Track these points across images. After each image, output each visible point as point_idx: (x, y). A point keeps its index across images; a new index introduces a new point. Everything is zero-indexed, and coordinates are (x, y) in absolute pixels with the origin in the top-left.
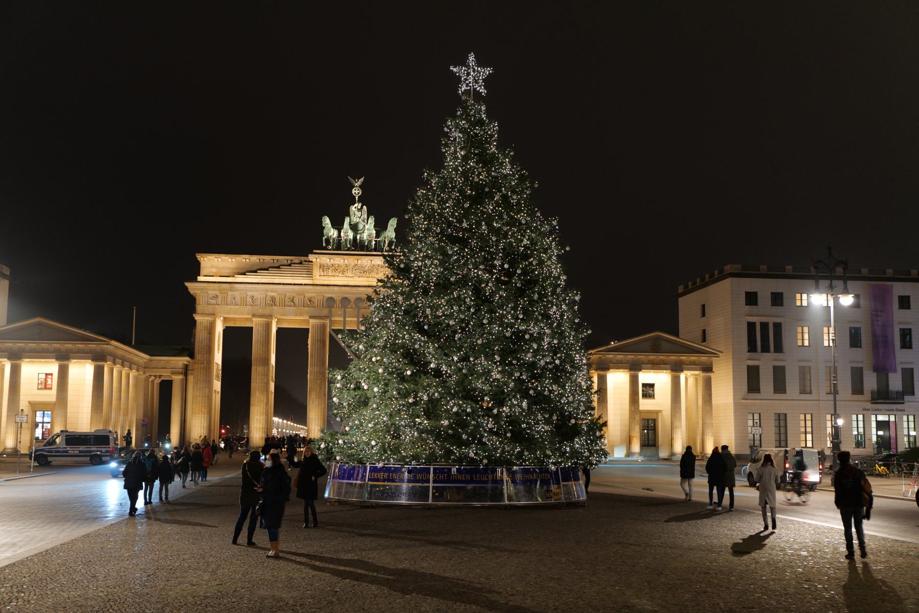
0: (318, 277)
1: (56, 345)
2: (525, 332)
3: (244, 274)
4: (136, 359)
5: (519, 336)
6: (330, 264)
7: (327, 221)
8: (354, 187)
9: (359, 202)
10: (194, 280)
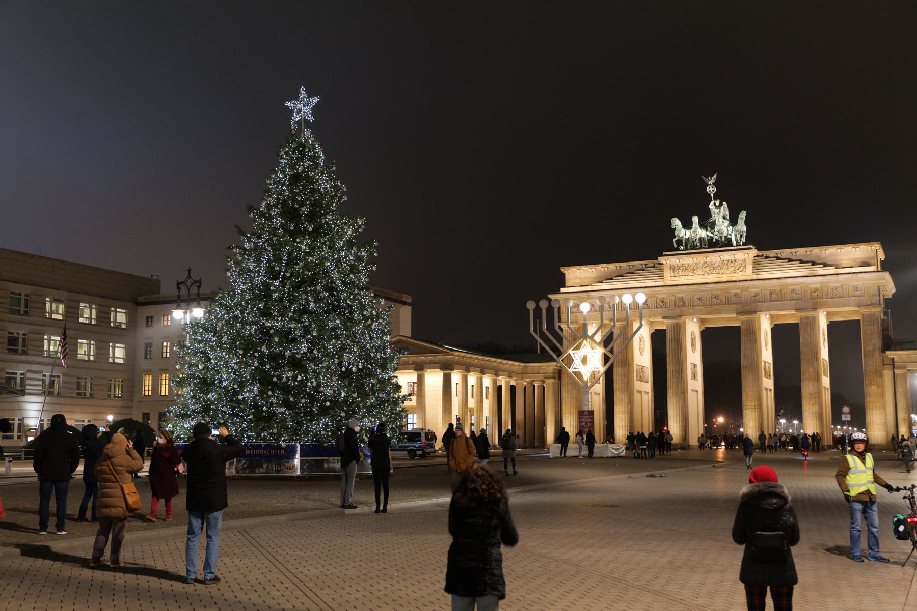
0: (669, 278)
1: (413, 358)
2: (271, 327)
3: (602, 282)
4: (505, 366)
5: (265, 332)
6: (679, 264)
7: (676, 223)
8: (707, 185)
9: (715, 199)
10: (559, 292)
